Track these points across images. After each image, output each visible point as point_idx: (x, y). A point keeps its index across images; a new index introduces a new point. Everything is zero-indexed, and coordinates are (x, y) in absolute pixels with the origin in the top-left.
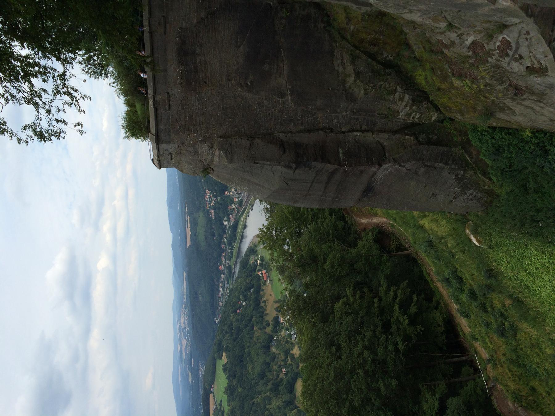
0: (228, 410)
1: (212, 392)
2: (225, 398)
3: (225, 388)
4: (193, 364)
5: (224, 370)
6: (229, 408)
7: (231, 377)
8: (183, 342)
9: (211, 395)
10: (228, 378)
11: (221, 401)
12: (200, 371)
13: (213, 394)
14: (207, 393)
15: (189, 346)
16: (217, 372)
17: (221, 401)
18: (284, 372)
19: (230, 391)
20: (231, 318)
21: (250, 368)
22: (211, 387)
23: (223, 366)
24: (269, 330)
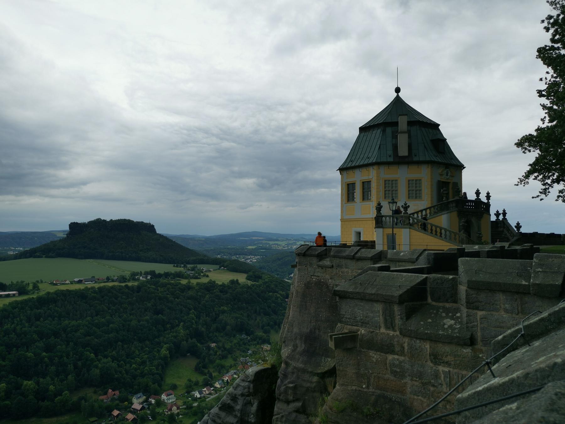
0: (193, 284)
1: (220, 267)
2: (204, 280)
3: (214, 282)
4: (261, 250)
5: (232, 282)
6: (195, 283)
7: (223, 288)
8: (284, 242)
9: (218, 266)
10: (223, 285)
11: (207, 276)
12: (254, 256)
13: (218, 269)
14: (220, 264)
15: (278, 247)
16: (235, 274)
17: (207, 276)
18: (210, 345)
19: (211, 287)
20: (281, 292)
21: (226, 308)
22: (224, 268)
23: (237, 280)
24: (260, 333)
